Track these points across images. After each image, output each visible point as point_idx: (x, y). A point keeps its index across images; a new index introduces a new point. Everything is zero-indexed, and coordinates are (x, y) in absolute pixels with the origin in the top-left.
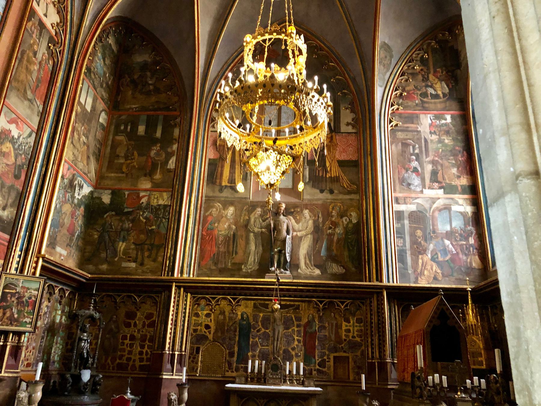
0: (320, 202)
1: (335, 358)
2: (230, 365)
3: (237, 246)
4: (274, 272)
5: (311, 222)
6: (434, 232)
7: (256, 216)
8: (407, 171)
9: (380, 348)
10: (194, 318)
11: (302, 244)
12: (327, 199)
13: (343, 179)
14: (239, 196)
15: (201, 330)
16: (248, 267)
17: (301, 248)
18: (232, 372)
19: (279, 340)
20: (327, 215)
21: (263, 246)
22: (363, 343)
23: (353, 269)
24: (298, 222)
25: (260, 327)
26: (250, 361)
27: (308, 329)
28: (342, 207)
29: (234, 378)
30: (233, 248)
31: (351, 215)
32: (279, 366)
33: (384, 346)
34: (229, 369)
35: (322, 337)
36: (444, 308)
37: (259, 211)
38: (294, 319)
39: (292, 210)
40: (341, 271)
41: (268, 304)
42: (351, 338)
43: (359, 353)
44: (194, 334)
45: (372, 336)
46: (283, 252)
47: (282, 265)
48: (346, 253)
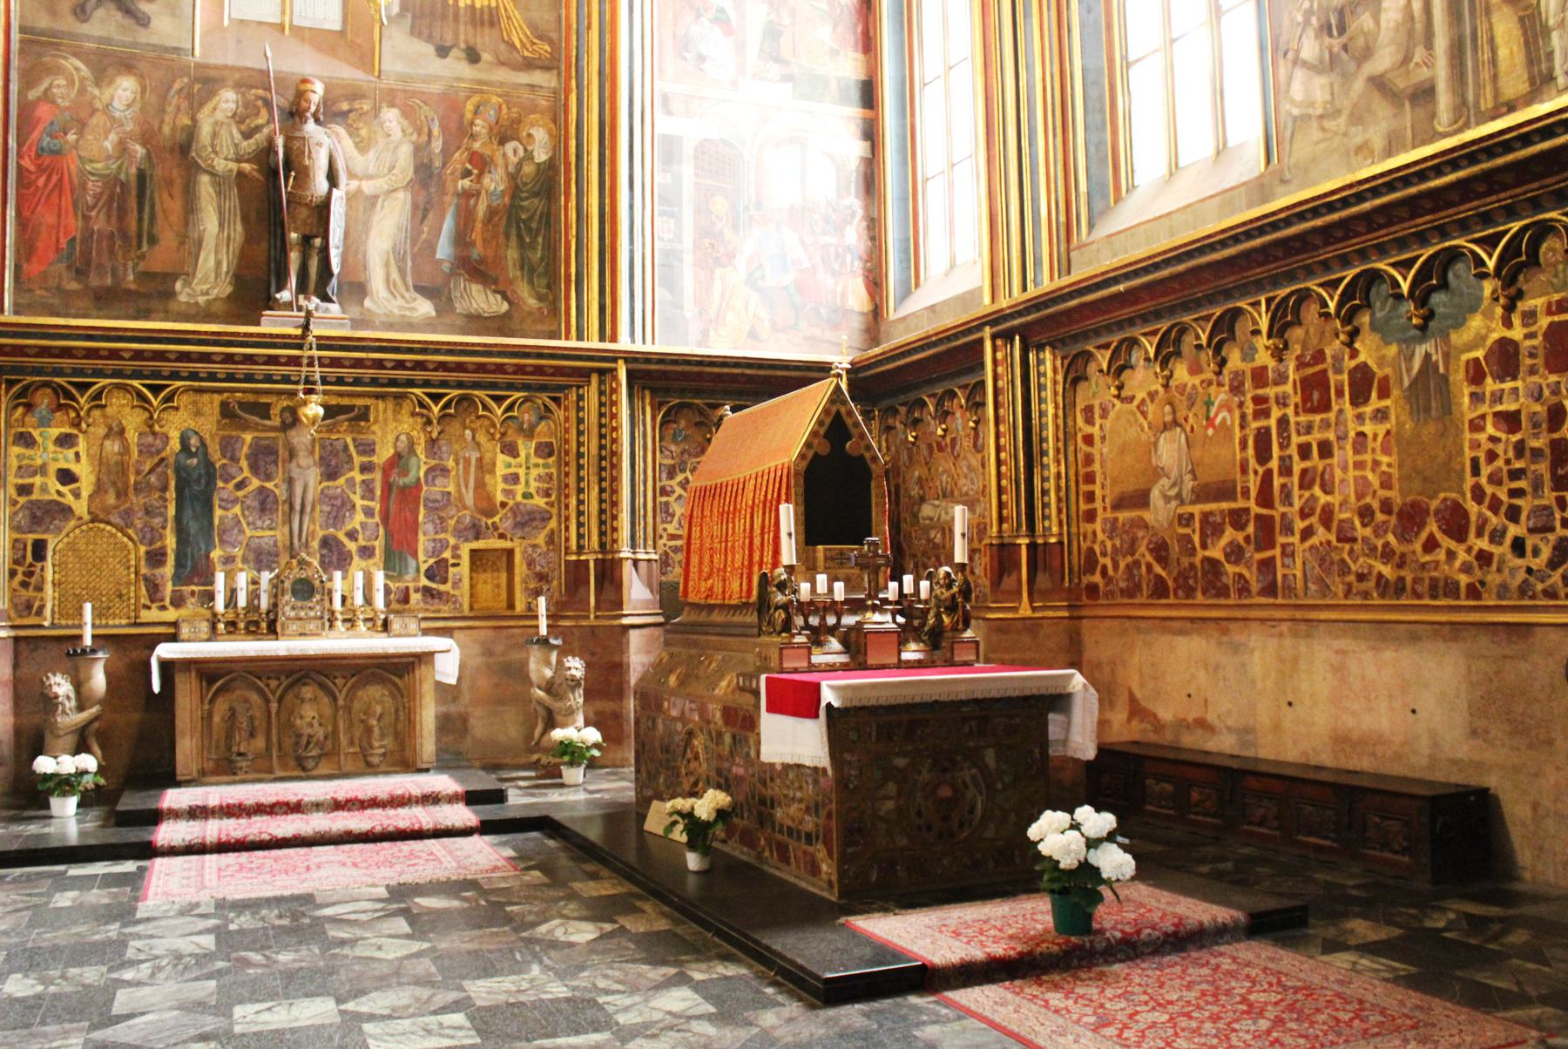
0: (436, 88)
1: (474, 553)
2: (154, 589)
3: (153, 218)
4: (288, 306)
5: (406, 151)
6: (759, 204)
7: (219, 116)
8: (698, 16)
9: (602, 523)
10: (16, 450)
11: (376, 218)
12: (460, 79)
13: (509, 18)
14: (154, 40)
15: (44, 489)
16: (198, 288)
17: (373, 233)
18: (163, 608)
19: (308, 509)
20: (459, 132)
21: (245, 219)
22: (554, 511)
23: (532, 302)
24: (362, 146)
25: (247, 473)
26: (220, 578)
27: (394, 477)
28: (504, 111)
29: (175, 624)
30: (140, 220)
31: (530, 135)
32: (317, 583)
33: (614, 517)
34: (152, 601)
35: (439, 497)
36: (843, 410)
37: (228, 100)
38: (352, 448)
39: (345, 106)
40: (495, 308)
41: (268, 405)
42: (519, 498)
43: (541, 539)
44: (22, 500)
45: (580, 491)
46: (318, 242)
47: (312, 285)
48: (512, 254)
